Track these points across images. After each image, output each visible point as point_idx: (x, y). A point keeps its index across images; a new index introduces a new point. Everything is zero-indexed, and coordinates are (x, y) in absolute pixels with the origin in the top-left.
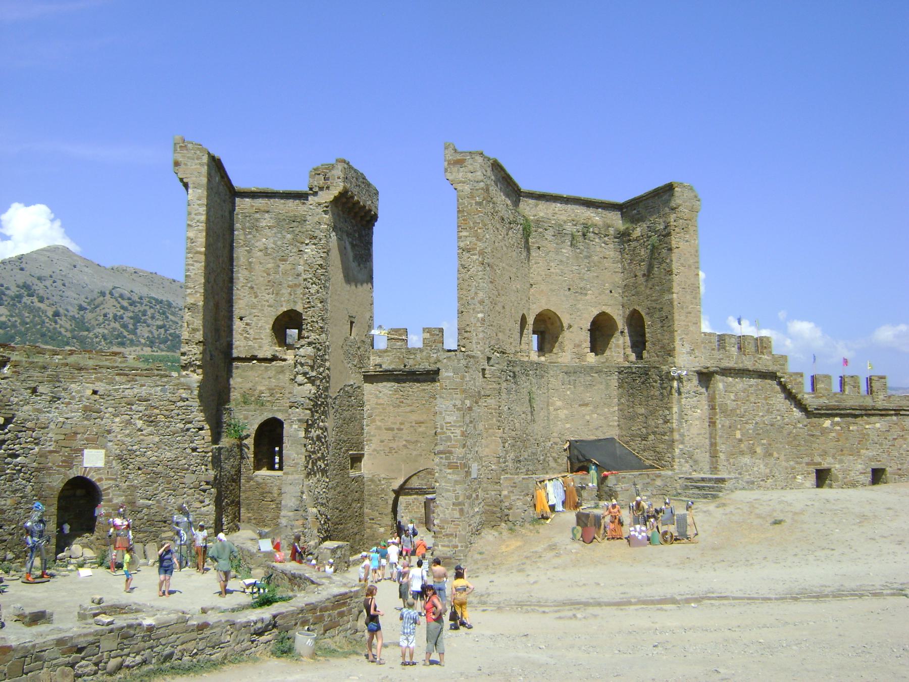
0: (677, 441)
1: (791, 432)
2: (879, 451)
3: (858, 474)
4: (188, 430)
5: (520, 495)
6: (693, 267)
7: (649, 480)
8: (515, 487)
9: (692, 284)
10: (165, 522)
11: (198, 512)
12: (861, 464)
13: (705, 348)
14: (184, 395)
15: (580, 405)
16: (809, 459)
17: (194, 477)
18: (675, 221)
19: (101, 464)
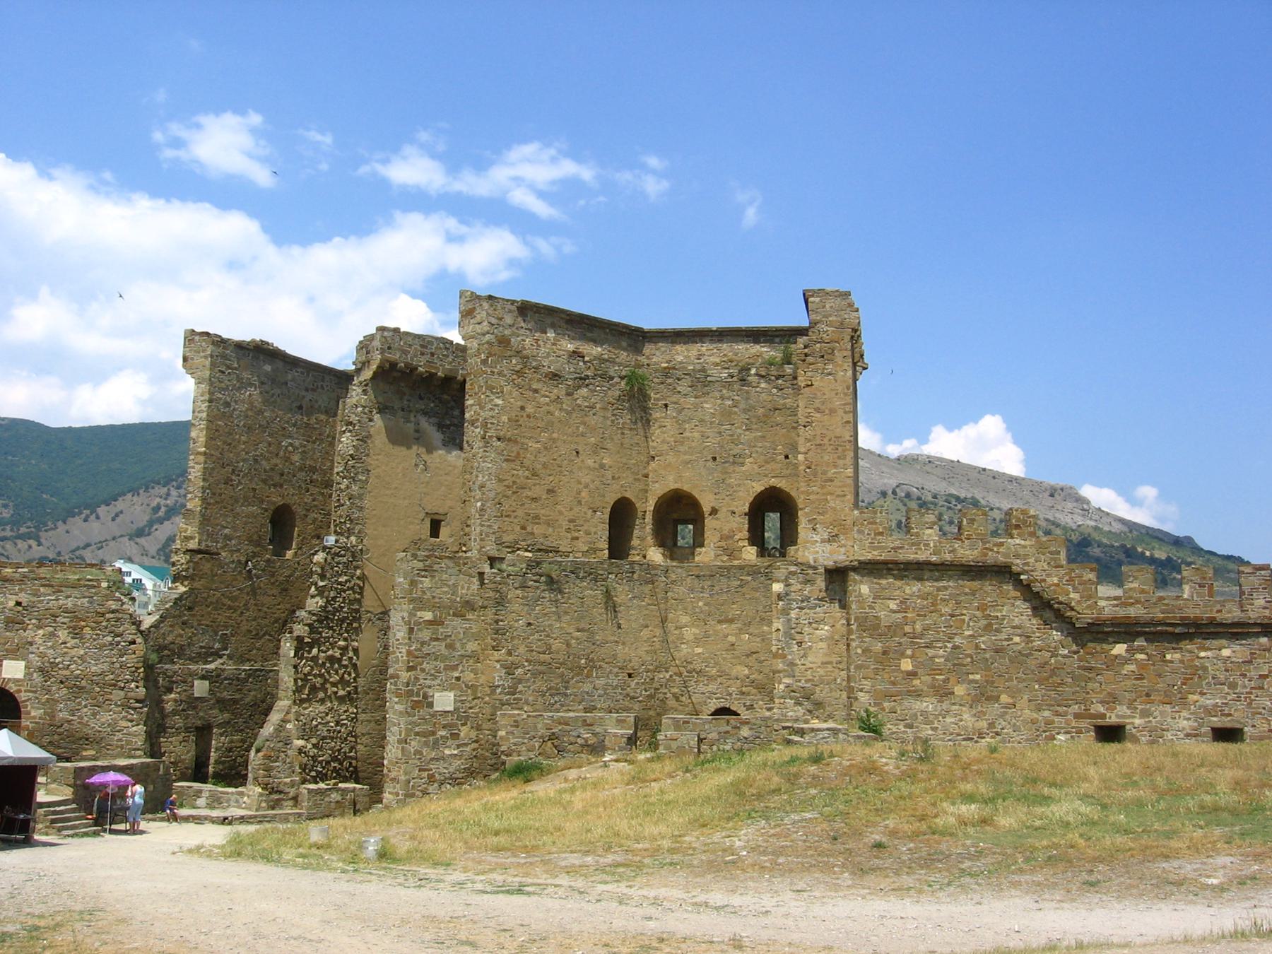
0: (779, 672)
1: (1046, 663)
2: (1229, 697)
3: (1182, 736)
4: (118, 643)
5: (524, 738)
6: (840, 412)
7: (729, 728)
8: (517, 726)
9: (835, 437)
10: (87, 739)
11: (125, 732)
12: (1190, 719)
13: (860, 532)
14: (113, 607)
15: (719, 622)
16: (1079, 707)
17: (122, 693)
18: (805, 347)
19: (20, 675)
